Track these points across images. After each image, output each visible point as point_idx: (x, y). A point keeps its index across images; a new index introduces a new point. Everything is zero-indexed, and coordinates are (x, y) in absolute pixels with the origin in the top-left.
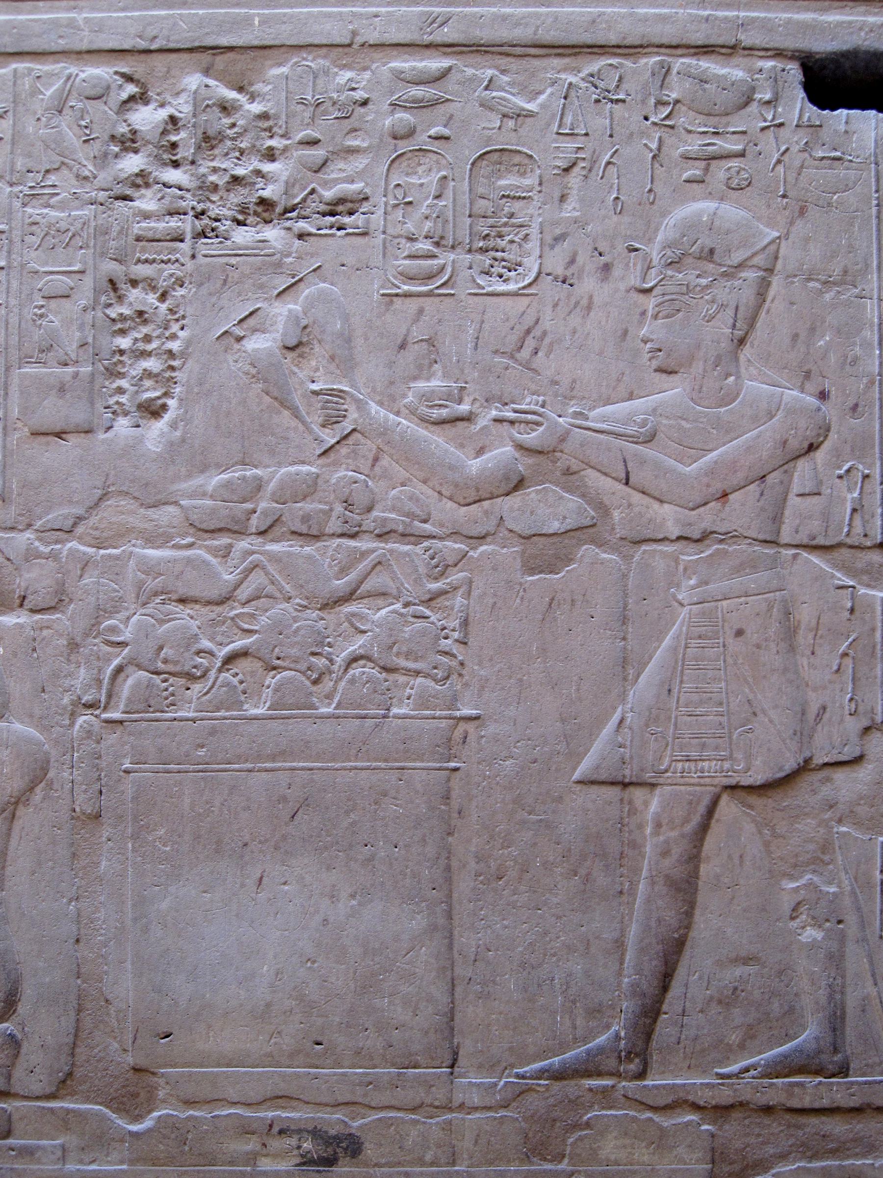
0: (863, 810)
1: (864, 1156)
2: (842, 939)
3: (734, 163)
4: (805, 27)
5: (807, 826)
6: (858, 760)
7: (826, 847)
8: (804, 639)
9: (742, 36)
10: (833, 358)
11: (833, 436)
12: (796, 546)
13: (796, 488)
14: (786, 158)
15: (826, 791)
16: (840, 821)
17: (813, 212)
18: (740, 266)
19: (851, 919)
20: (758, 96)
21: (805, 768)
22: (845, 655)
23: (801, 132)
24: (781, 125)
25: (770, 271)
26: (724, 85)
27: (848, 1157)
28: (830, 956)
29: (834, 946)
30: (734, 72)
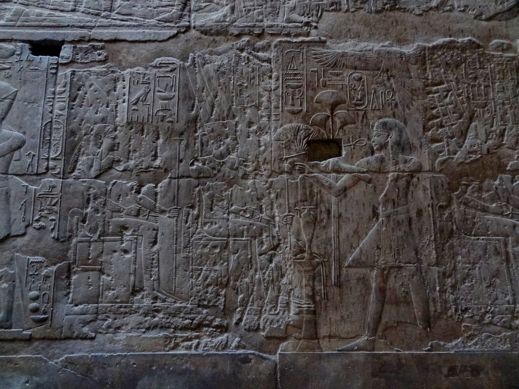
0: (24, 249)
1: (14, 355)
2: (14, 286)
3: (7, 71)
4: (32, 34)
5: (7, 254)
6: (24, 235)
7: (12, 259)
8: (12, 200)
9: (13, 37)
10: (28, 123)
11: (26, 144)
12: (12, 175)
13: (14, 158)
14: (22, 69)
15: (14, 243)
16: (17, 252)
17: (28, 83)
18: (5, 98)
19: (17, 281)
20: (16, 53)
21: (8, 237)
22: (22, 205)
23: (27, 62)
24: (22, 60)
25: (13, 100)
26: (7, 49)
27: (9, 355)
28: (9, 292)
29: (11, 288)
30: (10, 46)
